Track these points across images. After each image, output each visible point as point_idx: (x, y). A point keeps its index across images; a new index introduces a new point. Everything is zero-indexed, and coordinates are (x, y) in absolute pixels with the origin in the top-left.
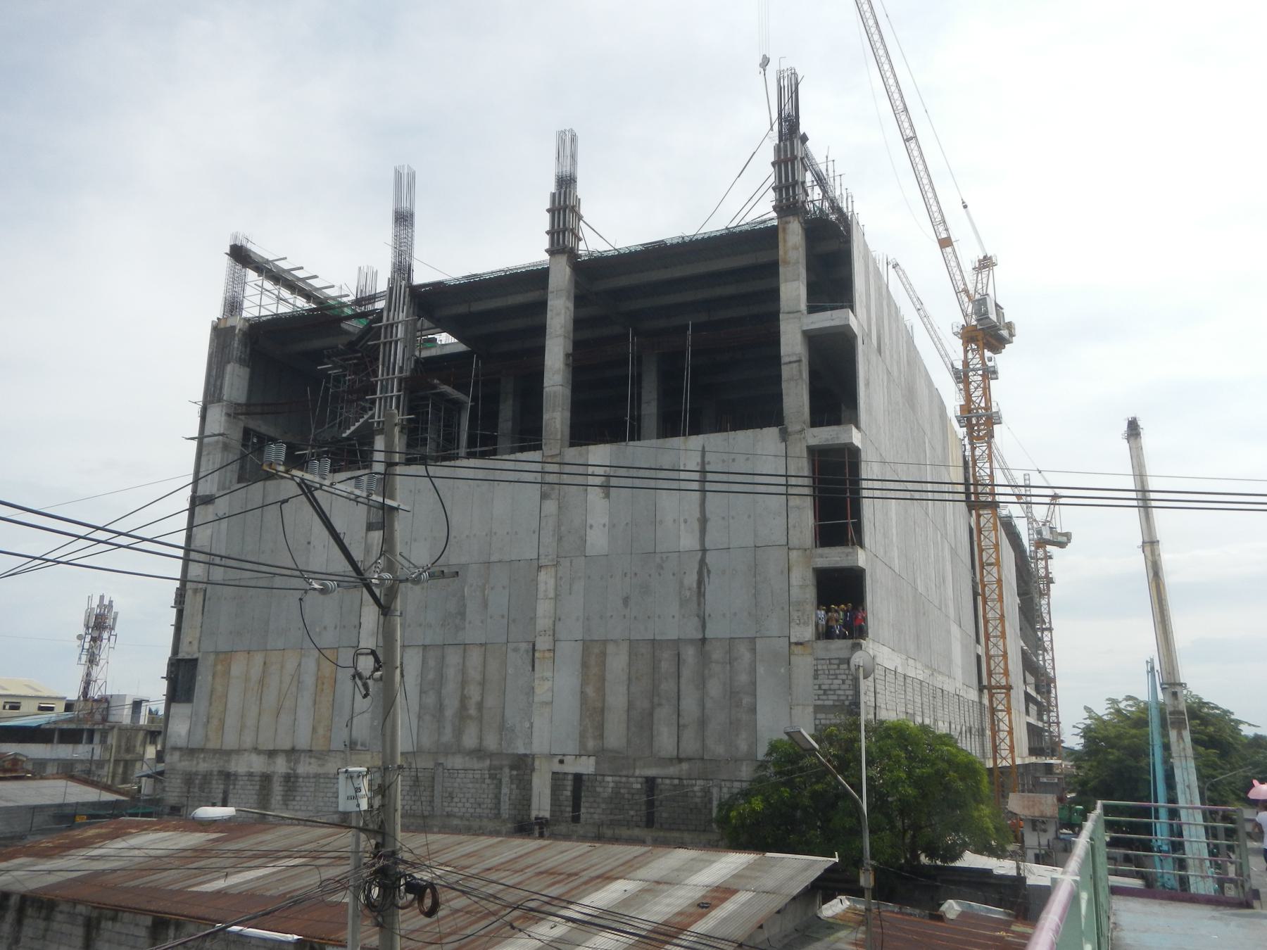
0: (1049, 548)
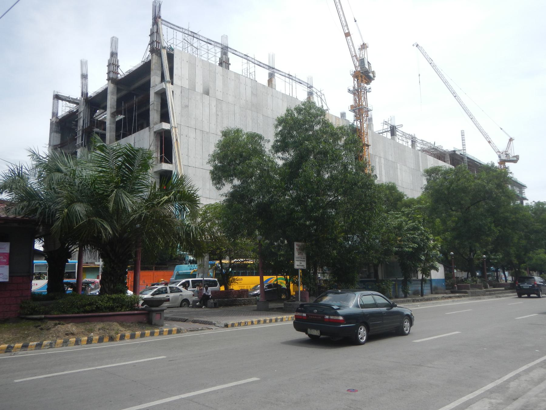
0: (507, 164)
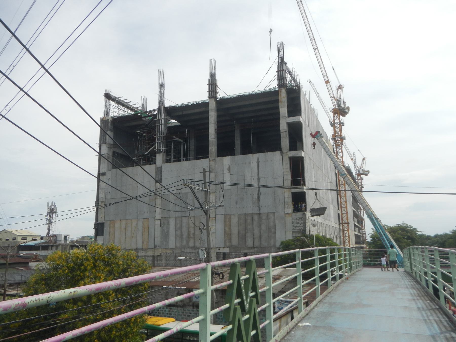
0: (362, 176)
